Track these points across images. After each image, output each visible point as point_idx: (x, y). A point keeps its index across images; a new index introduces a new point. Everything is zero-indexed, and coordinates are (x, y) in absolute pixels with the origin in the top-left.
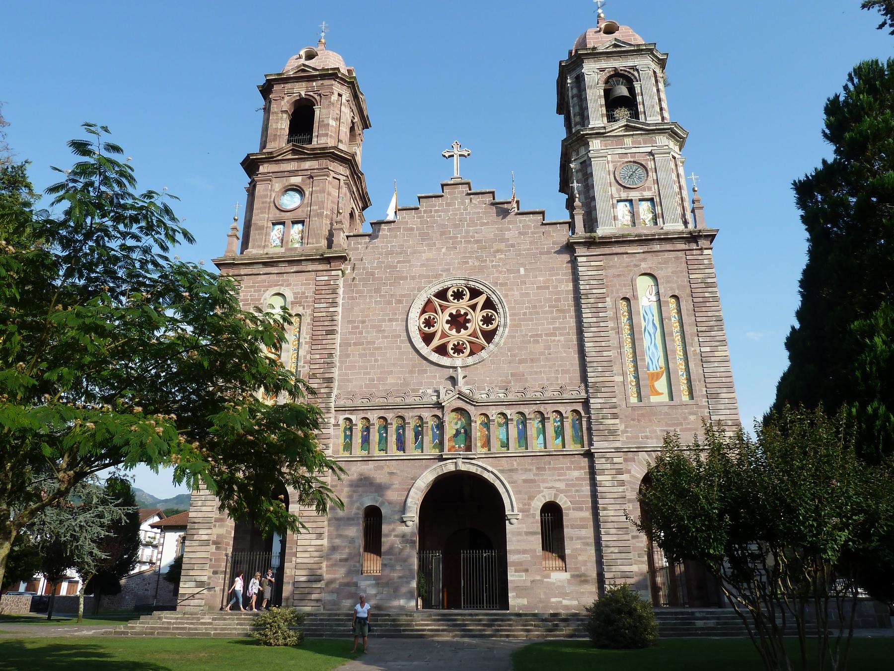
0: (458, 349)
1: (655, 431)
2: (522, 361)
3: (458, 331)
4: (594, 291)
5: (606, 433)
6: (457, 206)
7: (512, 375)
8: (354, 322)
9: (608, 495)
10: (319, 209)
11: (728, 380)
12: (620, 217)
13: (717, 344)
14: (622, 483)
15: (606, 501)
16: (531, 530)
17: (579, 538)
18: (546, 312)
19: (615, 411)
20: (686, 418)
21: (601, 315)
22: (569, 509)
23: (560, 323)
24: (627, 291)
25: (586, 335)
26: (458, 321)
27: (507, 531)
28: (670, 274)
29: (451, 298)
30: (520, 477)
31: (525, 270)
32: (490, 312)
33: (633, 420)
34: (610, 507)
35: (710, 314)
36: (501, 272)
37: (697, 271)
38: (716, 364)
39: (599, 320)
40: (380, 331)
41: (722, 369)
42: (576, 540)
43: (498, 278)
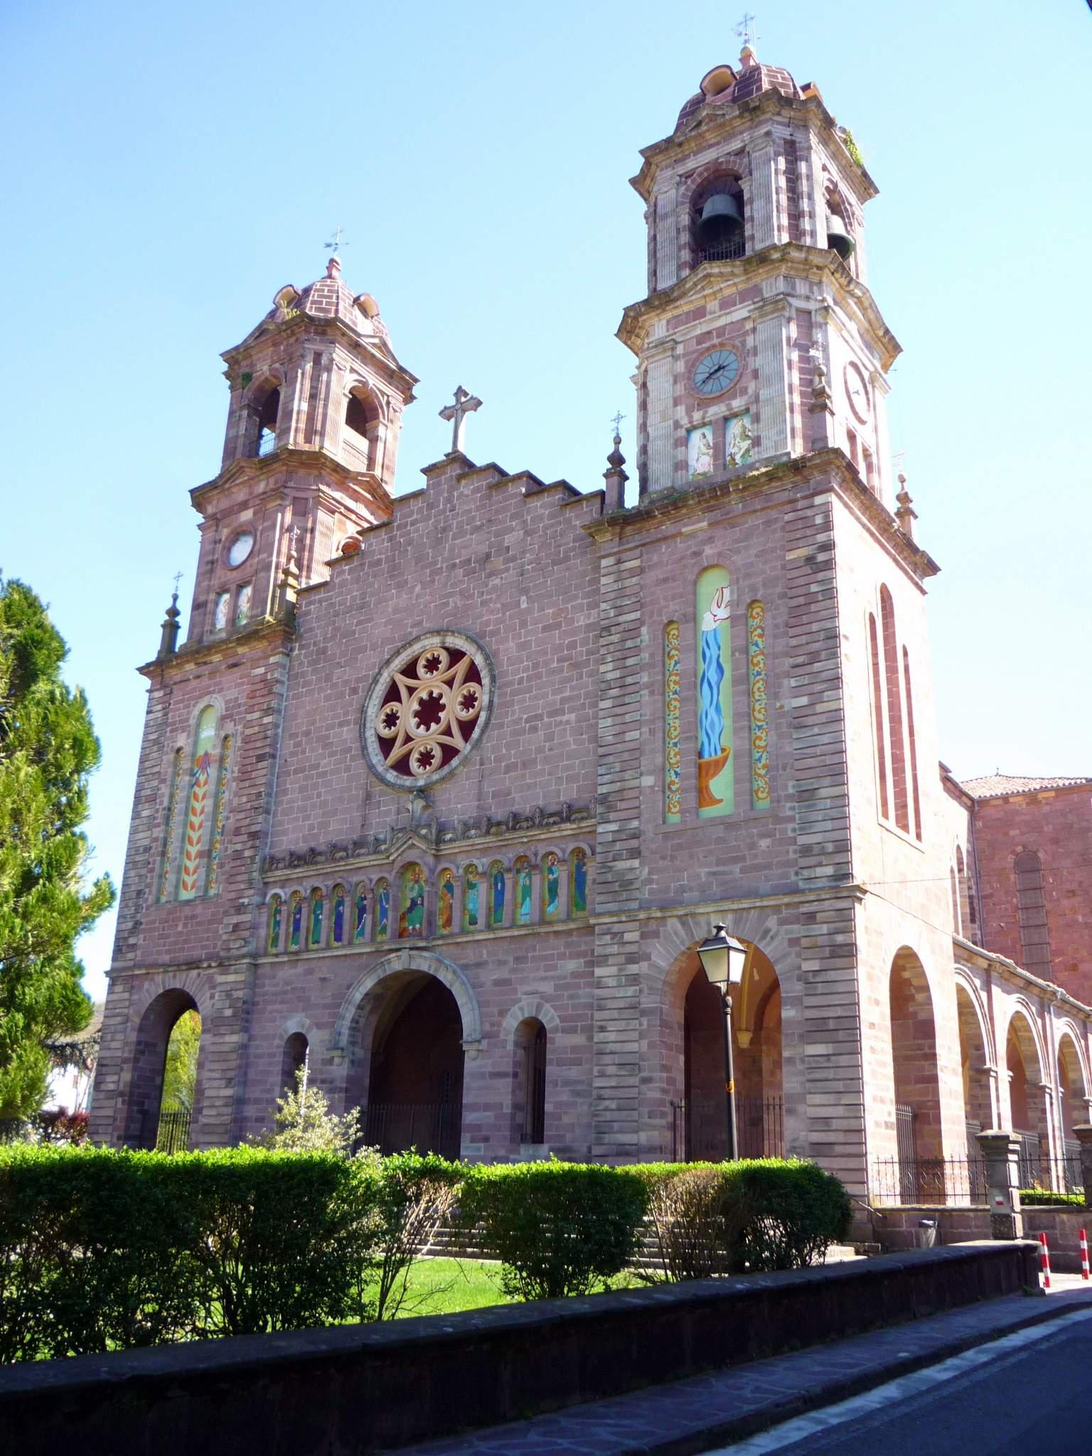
1: (699, 876)
2: (508, 769)
8: (296, 735)
9: (610, 1004)
11: (835, 759)
12: (692, 462)
13: (824, 686)
14: (634, 979)
15: (606, 1015)
16: (497, 1070)
17: (567, 1083)
18: (553, 672)
19: (634, 843)
20: (752, 846)
21: (630, 662)
22: (556, 1030)
23: (572, 688)
24: (677, 607)
27: (466, 1071)
28: (753, 559)
30: (490, 975)
31: (530, 600)
32: (473, 686)
35: (815, 627)
37: (801, 543)
38: (816, 730)
39: (625, 672)
40: (327, 744)
41: (826, 739)
42: (562, 1086)
43: (487, 623)
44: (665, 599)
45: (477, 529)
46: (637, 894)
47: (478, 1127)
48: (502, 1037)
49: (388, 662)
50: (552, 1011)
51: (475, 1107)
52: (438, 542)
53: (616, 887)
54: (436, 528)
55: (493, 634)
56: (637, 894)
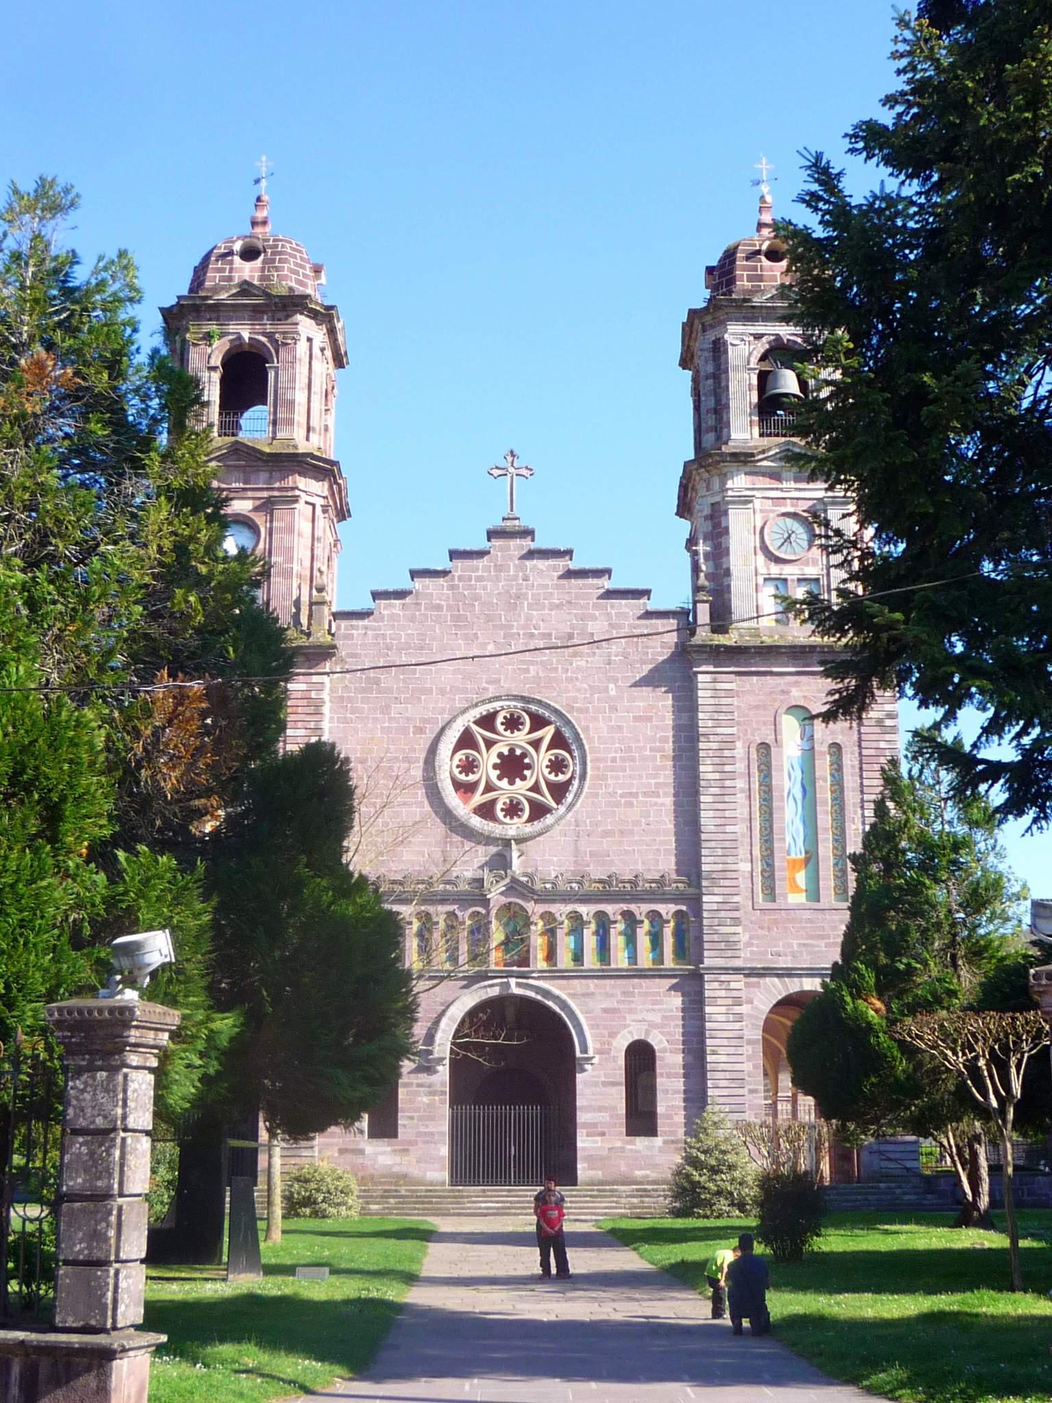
0: (513, 809)
1: (790, 945)
2: (607, 834)
3: (512, 783)
4: (720, 730)
5: (722, 946)
6: (512, 573)
7: (592, 854)
9: (719, 1034)
10: (286, 562)
14: (739, 1018)
18: (644, 759)
19: (736, 914)
21: (727, 768)
22: (664, 1050)
25: (703, 798)
26: (512, 766)
29: (501, 728)
30: (598, 1005)
33: (762, 928)
34: (721, 1050)
36: (579, 690)
39: (724, 776)
43: (575, 700)
44: (757, 722)
45: (559, 607)
46: (737, 953)
47: (595, 1125)
48: (613, 1053)
49: (464, 711)
50: (661, 1037)
51: (590, 1109)
52: (512, 607)
53: (722, 946)
54: (508, 592)
55: (580, 710)
56: (737, 953)
